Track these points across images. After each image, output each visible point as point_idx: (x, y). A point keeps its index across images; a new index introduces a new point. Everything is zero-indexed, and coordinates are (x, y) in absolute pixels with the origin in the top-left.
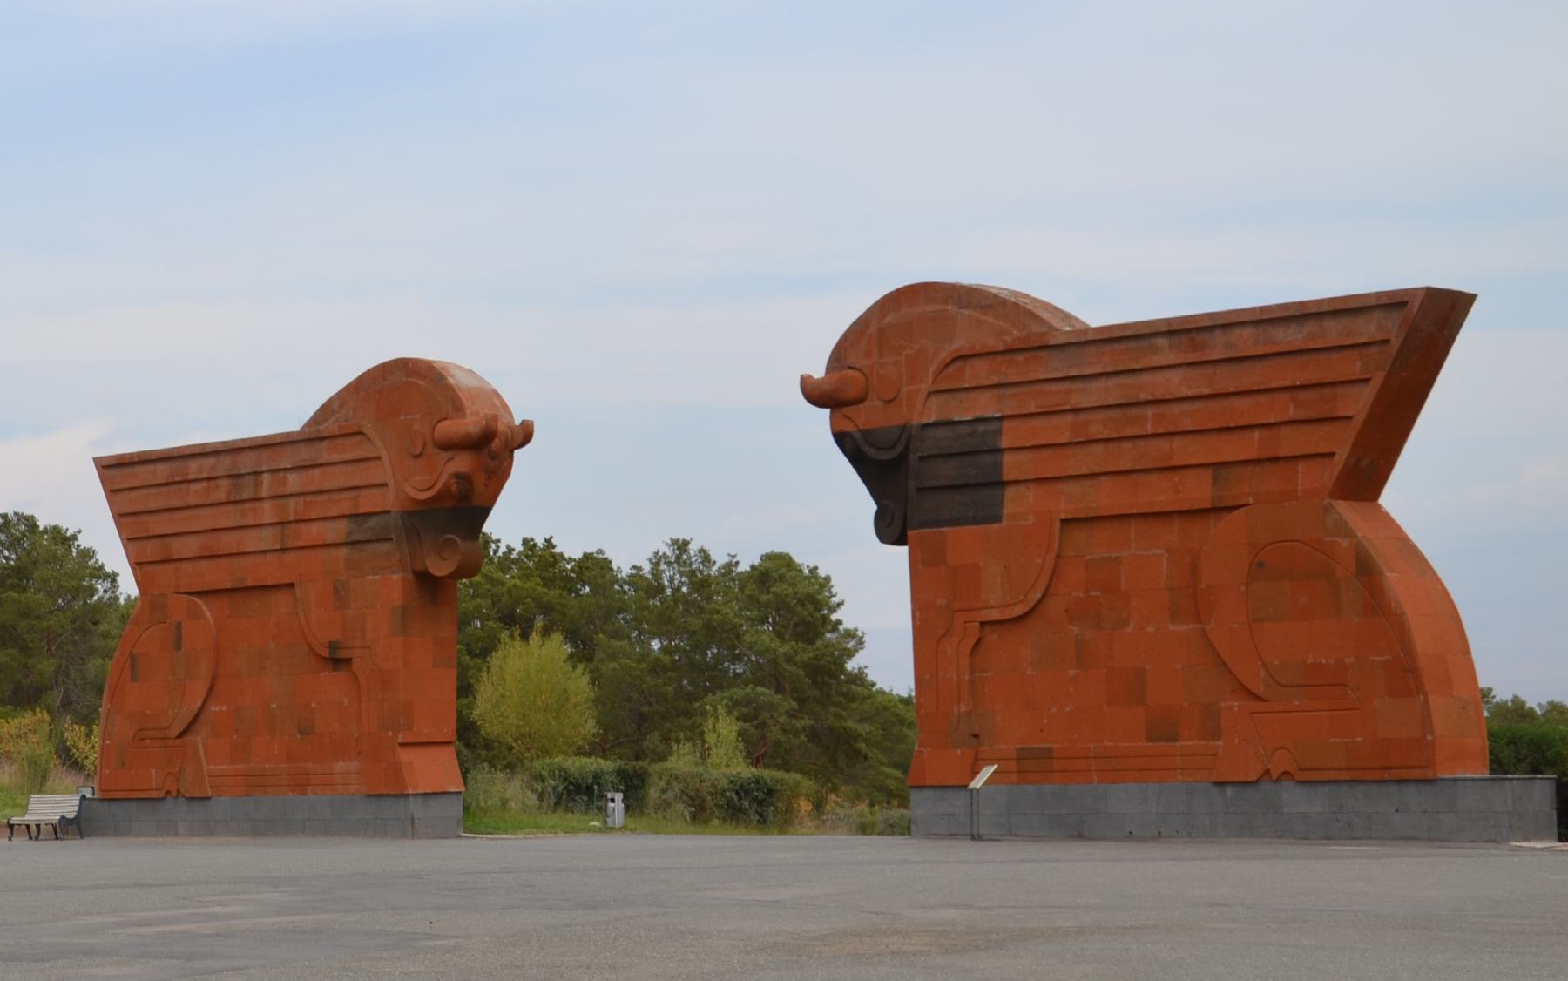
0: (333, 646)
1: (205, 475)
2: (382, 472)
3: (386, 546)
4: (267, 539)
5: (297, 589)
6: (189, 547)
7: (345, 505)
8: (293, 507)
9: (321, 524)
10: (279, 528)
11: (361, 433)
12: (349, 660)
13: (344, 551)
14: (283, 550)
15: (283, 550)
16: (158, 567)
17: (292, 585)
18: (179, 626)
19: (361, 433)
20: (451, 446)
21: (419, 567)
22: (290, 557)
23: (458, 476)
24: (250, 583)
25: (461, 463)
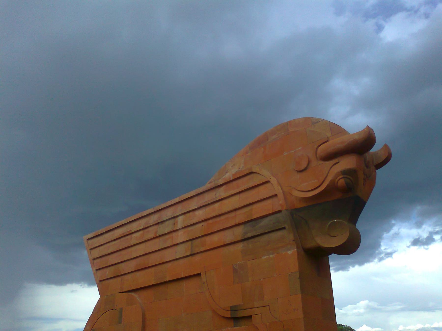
0: (233, 309)
1: (142, 227)
2: (275, 188)
3: (279, 233)
4: (181, 251)
5: (203, 276)
6: (132, 266)
7: (241, 216)
8: (198, 230)
9: (221, 233)
10: (189, 243)
11: (252, 173)
12: (250, 317)
13: (241, 245)
14: (192, 255)
15: (192, 255)
16: (111, 281)
17: (199, 275)
18: (122, 309)
19: (252, 173)
20: (331, 157)
21: (310, 244)
22: (197, 258)
23: (345, 173)
24: (167, 279)
25: (347, 163)
